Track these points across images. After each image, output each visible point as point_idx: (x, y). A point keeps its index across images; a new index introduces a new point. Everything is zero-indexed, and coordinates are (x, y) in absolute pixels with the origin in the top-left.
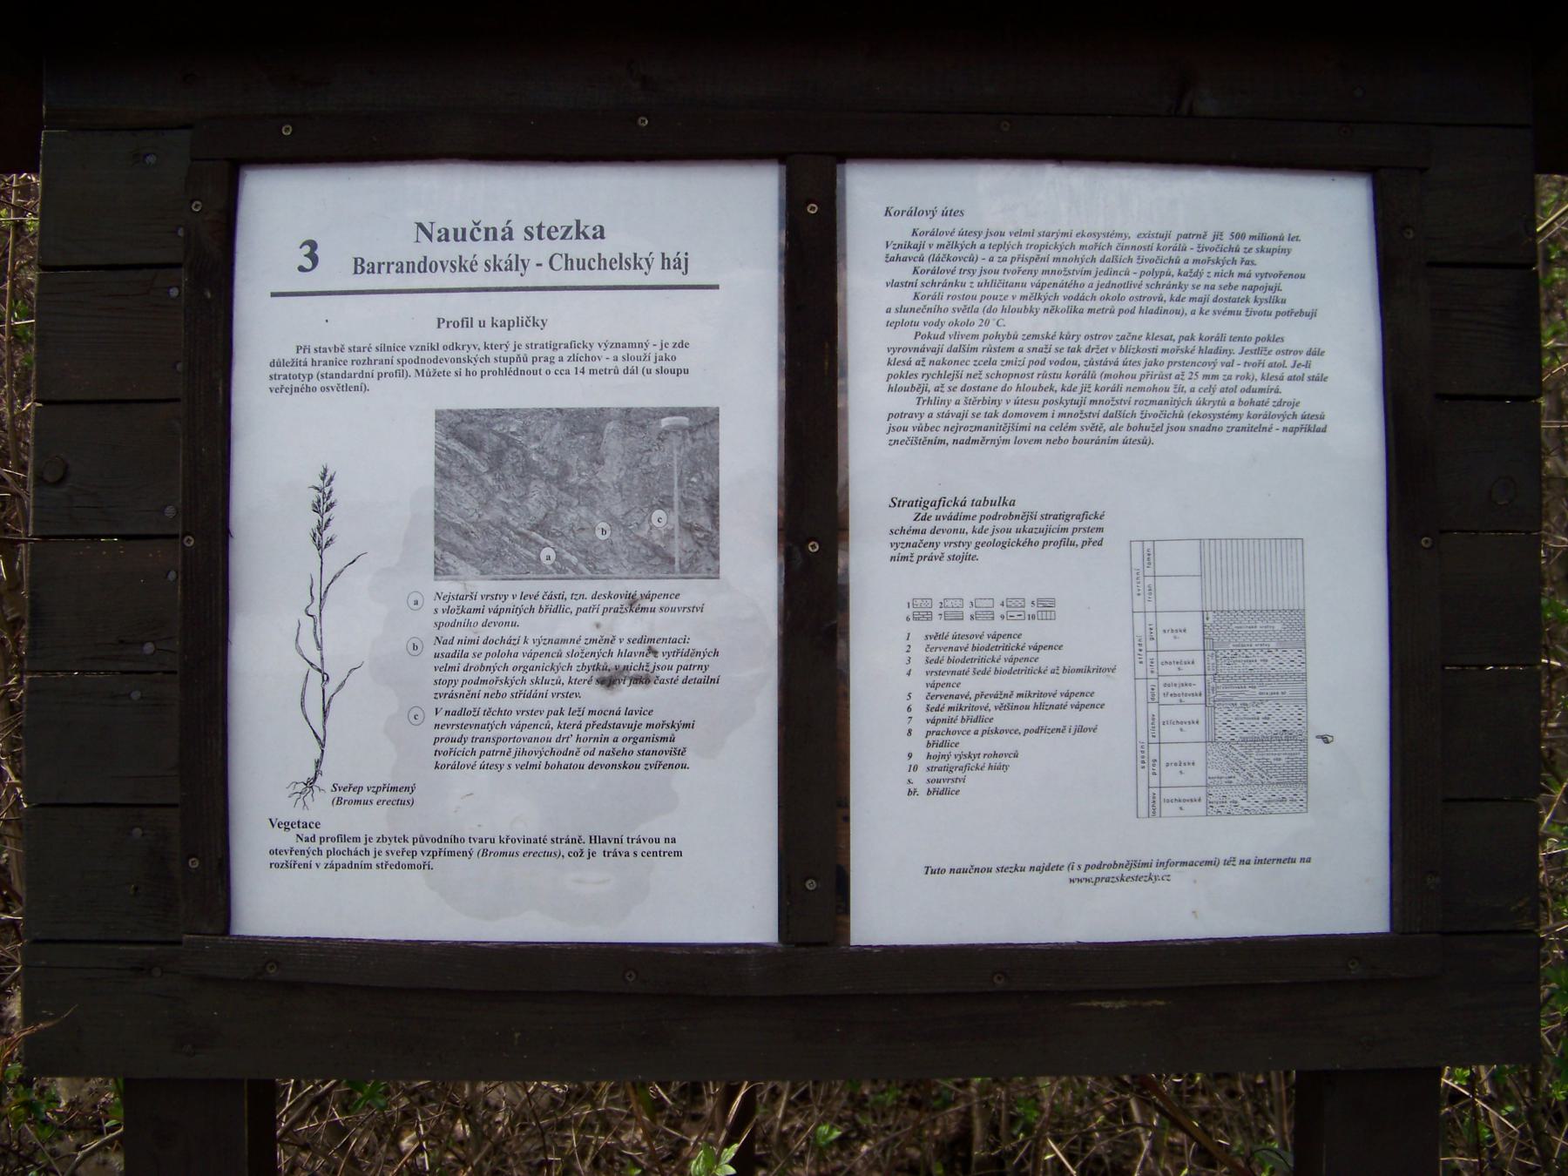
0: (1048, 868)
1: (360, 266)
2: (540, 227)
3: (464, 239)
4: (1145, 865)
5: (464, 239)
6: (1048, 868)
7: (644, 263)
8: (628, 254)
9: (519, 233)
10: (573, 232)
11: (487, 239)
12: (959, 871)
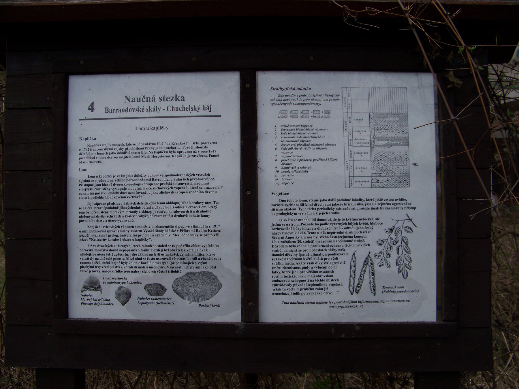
0: (323, 303)
1: (107, 110)
2: (164, 97)
3: (140, 101)
4: (355, 302)
5: (140, 101)
6: (323, 303)
8: (192, 106)
9: (157, 99)
10: (174, 99)
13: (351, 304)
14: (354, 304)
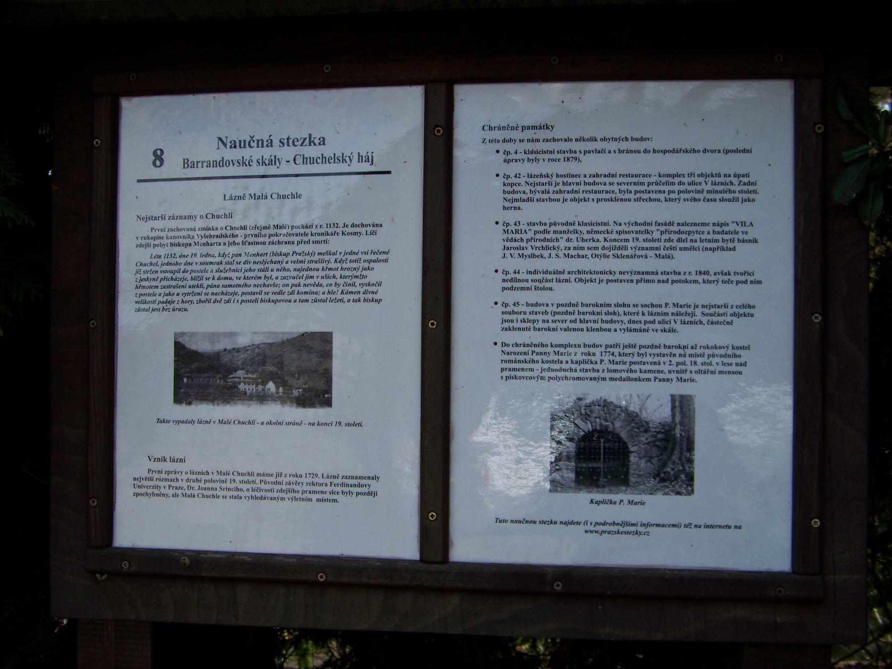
0: (572, 523)
1: (187, 164)
2: (288, 139)
3: (245, 147)
4: (633, 525)
5: (245, 147)
6: (572, 523)
7: (347, 159)
8: (339, 154)
9: (276, 143)
10: (307, 141)
11: (258, 147)
12: (516, 522)
13: (627, 529)
14: (633, 529)
